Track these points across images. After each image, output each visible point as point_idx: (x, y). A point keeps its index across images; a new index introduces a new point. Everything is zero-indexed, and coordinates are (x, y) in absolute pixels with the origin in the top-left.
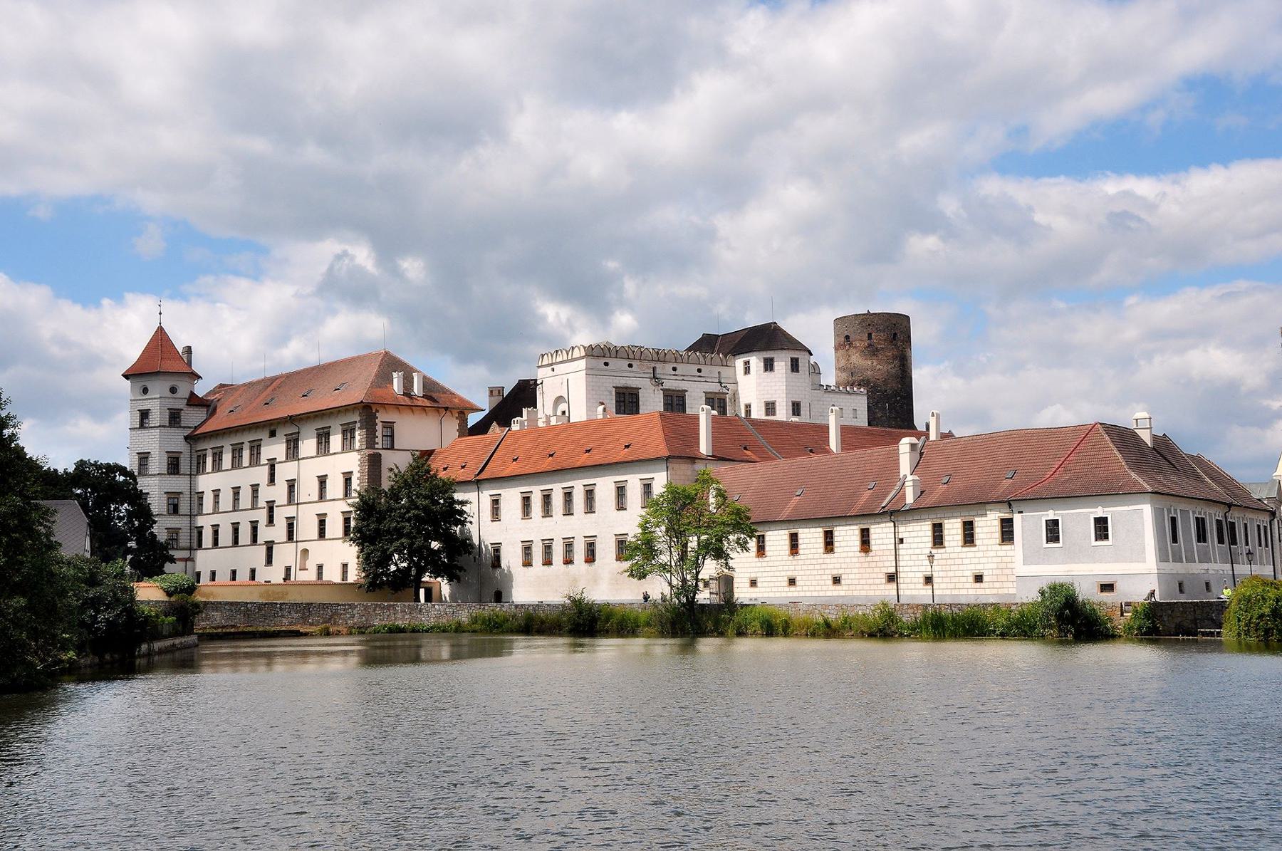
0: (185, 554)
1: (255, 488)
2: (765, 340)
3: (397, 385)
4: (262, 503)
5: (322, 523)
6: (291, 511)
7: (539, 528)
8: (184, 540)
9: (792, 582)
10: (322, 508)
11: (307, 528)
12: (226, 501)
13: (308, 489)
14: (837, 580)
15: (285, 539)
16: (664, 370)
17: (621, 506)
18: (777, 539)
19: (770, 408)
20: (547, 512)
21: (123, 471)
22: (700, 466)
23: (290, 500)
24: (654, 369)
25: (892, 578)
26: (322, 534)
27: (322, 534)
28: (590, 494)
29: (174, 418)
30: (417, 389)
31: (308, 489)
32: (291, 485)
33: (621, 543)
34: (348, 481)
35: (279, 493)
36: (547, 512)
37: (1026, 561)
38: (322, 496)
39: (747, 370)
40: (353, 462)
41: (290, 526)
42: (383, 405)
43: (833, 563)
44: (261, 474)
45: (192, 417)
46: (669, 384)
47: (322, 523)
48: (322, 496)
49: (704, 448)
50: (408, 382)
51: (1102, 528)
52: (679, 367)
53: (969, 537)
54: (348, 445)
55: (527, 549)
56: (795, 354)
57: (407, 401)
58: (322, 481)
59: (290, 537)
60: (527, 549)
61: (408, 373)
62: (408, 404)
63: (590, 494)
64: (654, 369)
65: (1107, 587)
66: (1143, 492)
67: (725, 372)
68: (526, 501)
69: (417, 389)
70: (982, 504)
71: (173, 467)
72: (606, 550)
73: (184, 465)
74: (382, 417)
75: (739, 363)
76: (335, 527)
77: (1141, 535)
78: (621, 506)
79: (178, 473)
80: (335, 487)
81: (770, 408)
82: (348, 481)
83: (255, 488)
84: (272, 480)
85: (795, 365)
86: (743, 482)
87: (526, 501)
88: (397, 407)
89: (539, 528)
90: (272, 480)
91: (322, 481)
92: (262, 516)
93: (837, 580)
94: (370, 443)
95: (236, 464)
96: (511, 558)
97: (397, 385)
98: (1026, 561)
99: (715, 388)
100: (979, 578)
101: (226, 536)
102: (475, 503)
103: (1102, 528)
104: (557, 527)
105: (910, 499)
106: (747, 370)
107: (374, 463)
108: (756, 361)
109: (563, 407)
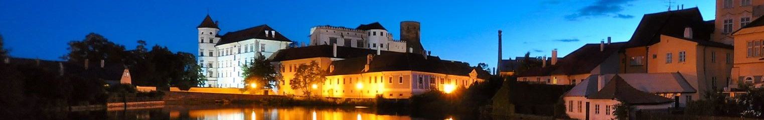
0: (215, 79)
8: (214, 75)
12: (225, 66)
19: (375, 45)
21: (192, 55)
22: (332, 59)
24: (342, 33)
29: (211, 41)
33: (291, 81)
45: (217, 40)
46: (345, 37)
49: (335, 56)
50: (270, 33)
52: (349, 32)
53: (376, 82)
54: (252, 51)
56: (382, 31)
61: (270, 30)
62: (270, 37)
64: (342, 33)
65: (401, 95)
67: (363, 34)
71: (211, 54)
73: (214, 54)
79: (212, 56)
85: (382, 34)
101: (224, 75)
105: (366, 71)
108: (372, 31)
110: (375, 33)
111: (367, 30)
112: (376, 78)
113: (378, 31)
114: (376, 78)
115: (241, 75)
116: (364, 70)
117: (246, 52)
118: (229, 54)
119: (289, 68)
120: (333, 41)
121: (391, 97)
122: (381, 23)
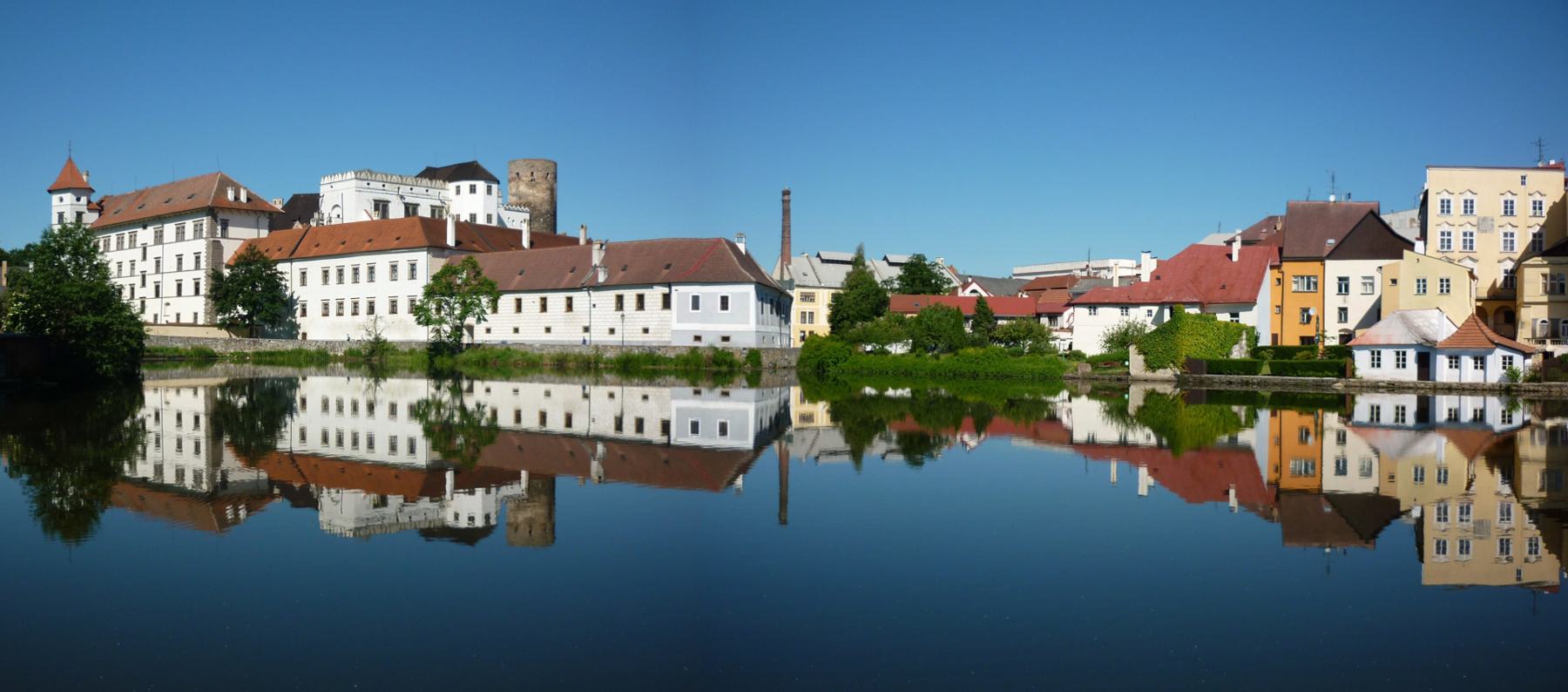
1: (133, 263)
2: (468, 171)
3: (230, 195)
4: (137, 272)
5: (179, 286)
6: (158, 278)
7: (333, 292)
9: (516, 330)
10: (179, 276)
11: (169, 289)
13: (169, 263)
14: (548, 330)
15: (153, 294)
16: (404, 190)
17: (413, 276)
18: (506, 302)
20: (340, 280)
23: (157, 271)
25: (586, 329)
26: (179, 293)
27: (179, 293)
28: (371, 270)
30: (243, 198)
31: (169, 263)
32: (158, 263)
34: (198, 258)
35: (149, 266)
36: (340, 280)
37: (679, 321)
38: (179, 269)
39: (458, 192)
40: (201, 246)
41: (157, 288)
42: (222, 209)
43: (546, 319)
44: (138, 253)
46: (408, 200)
47: (179, 286)
48: (179, 269)
51: (724, 302)
55: (326, 306)
57: (236, 205)
58: (180, 259)
59: (157, 295)
60: (326, 306)
63: (371, 270)
65: (726, 339)
66: (750, 282)
68: (326, 273)
69: (243, 198)
70: (650, 285)
72: (403, 306)
74: (221, 216)
75: (452, 186)
76: (188, 288)
77: (748, 308)
78: (413, 276)
80: (189, 262)
81: (473, 217)
82: (198, 258)
83: (133, 263)
84: (144, 258)
85: (489, 191)
86: (489, 262)
87: (326, 273)
88: (230, 210)
89: (333, 292)
90: (144, 258)
91: (180, 259)
92: (137, 281)
93: (548, 330)
94: (213, 233)
95: (120, 246)
96: (314, 309)
97: (230, 195)
98: (679, 321)
99: (438, 203)
100: (646, 331)
102: (289, 272)
103: (724, 302)
104: (348, 291)
105: (601, 278)
106: (458, 192)
107: (216, 248)
108: (465, 185)
109: (338, 211)
110: (473, 190)
111: (451, 180)
112: (641, 298)
113: (481, 185)
114: (641, 298)
115: (203, 290)
116: (596, 277)
117: (180, 235)
118: (126, 245)
119: (320, 275)
120: (381, 206)
121: (697, 344)
122: (485, 164)
